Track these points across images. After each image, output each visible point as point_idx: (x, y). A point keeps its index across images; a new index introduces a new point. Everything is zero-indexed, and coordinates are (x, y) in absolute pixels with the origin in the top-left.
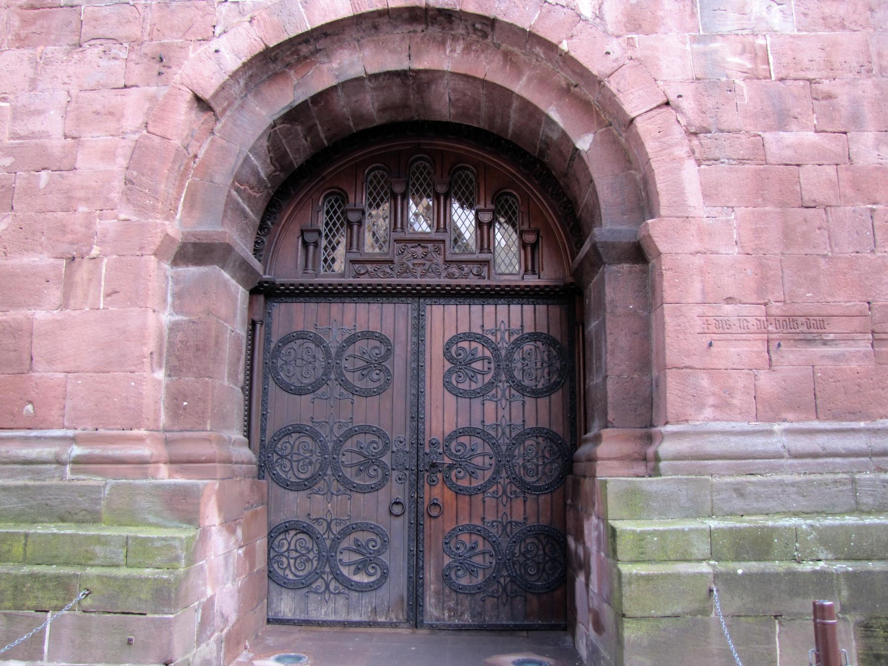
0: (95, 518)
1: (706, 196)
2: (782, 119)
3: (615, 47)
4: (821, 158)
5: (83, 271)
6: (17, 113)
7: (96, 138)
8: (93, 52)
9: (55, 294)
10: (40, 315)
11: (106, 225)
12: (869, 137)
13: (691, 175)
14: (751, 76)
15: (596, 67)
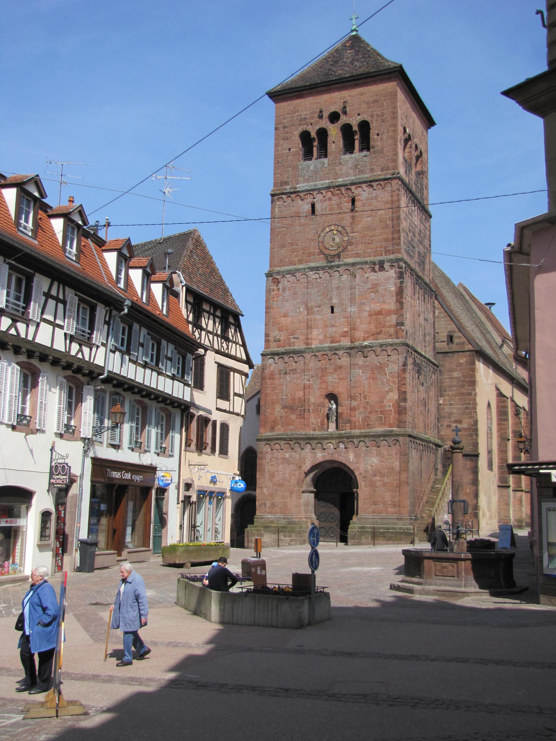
0: (296, 524)
1: (365, 486)
2: (375, 476)
3: (355, 466)
4: (379, 481)
5: (293, 495)
6: (283, 474)
7: (293, 478)
8: (291, 465)
9: (290, 498)
10: (288, 500)
11: (295, 489)
12: (386, 478)
13: (363, 483)
14: (372, 469)
15: (352, 469)
